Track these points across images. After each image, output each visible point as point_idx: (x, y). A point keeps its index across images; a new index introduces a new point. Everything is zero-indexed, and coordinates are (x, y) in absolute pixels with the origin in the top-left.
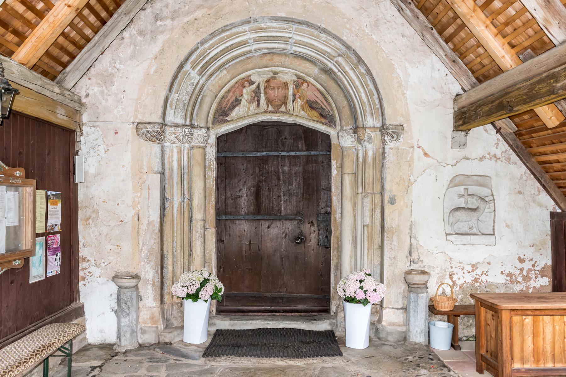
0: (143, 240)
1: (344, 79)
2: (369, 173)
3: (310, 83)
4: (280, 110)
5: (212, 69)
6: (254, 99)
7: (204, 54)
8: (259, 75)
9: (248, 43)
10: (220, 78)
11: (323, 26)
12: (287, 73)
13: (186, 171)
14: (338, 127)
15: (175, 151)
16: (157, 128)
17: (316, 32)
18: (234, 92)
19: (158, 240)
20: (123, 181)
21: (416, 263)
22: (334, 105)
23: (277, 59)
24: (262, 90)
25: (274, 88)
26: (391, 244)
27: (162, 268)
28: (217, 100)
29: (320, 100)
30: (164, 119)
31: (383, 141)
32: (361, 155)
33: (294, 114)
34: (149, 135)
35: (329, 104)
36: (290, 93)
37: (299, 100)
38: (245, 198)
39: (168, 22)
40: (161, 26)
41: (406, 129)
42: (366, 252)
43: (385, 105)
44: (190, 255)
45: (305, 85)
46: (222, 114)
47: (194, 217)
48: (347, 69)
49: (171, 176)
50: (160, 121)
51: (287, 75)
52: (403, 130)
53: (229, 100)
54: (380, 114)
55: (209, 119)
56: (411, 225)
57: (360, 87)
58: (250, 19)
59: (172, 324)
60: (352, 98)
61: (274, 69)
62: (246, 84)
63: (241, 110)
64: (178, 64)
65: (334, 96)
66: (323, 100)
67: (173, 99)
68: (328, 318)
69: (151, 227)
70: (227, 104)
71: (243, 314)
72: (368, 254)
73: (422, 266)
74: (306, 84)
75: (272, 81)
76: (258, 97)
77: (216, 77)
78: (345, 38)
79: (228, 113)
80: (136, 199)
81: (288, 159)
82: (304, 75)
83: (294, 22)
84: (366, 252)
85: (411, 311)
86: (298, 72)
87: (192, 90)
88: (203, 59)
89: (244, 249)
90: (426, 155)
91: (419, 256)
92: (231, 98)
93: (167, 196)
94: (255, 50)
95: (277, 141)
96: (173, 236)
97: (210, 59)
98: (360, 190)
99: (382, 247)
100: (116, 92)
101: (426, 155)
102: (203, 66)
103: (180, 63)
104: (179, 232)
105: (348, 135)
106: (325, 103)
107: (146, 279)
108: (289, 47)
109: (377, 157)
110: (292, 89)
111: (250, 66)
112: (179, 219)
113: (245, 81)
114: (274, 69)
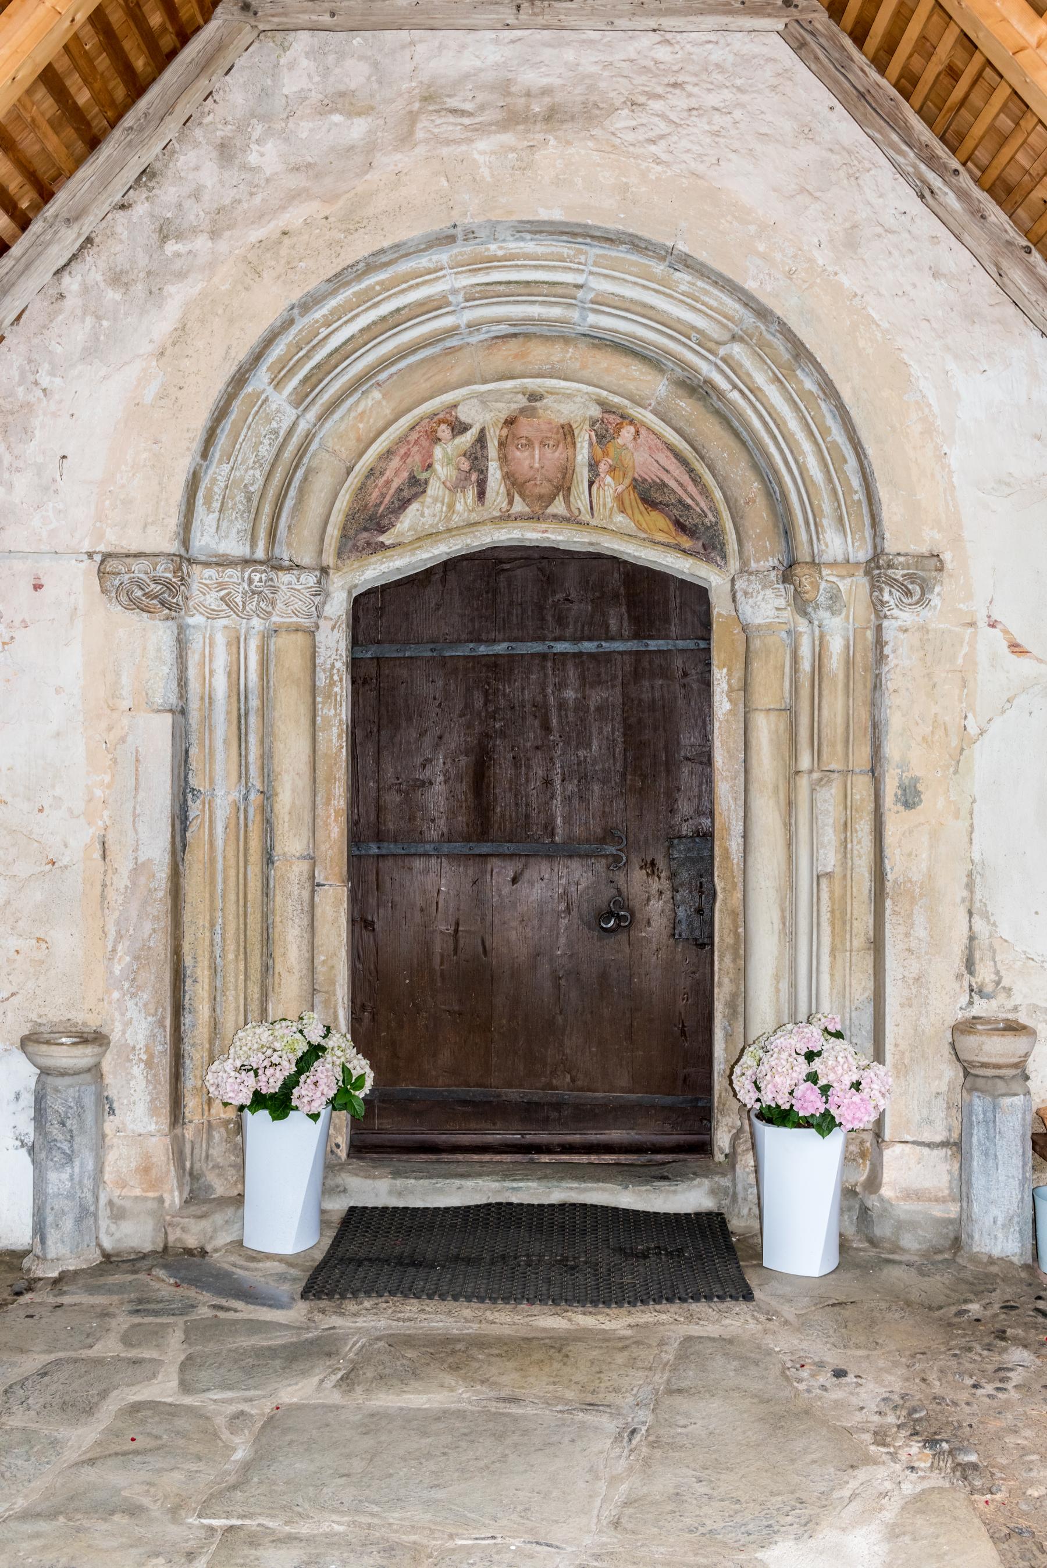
0: (118, 923)
1: (750, 412)
2: (834, 708)
3: (643, 424)
4: (552, 510)
6: (467, 479)
7: (311, 341)
8: (482, 402)
9: (449, 304)
10: (363, 412)
11: (682, 247)
12: (570, 396)
13: (254, 703)
14: (734, 564)
15: (220, 640)
16: (164, 570)
17: (659, 268)
18: (407, 455)
19: (166, 922)
20: (58, 734)
21: (988, 997)
22: (718, 495)
23: (539, 353)
24: (492, 451)
26: (907, 935)
27: (178, 1009)
29: (675, 477)
30: (186, 543)
31: (877, 606)
32: (805, 651)
33: (593, 522)
34: (139, 593)
35: (705, 491)
36: (579, 458)
37: (609, 479)
38: (439, 787)
39: (201, 243)
40: (178, 255)
41: (949, 565)
42: (826, 959)
43: (883, 493)
44: (267, 969)
46: (367, 527)
47: (278, 850)
48: (760, 379)
49: (207, 719)
50: (173, 547)
52: (940, 569)
53: (388, 482)
54: (867, 521)
55: (327, 540)
56: (970, 875)
57: (800, 436)
58: (452, 231)
59: (209, 1188)
60: (776, 472)
62: (444, 432)
63: (426, 511)
64: (229, 370)
65: (719, 465)
66: (685, 479)
67: (214, 481)
68: (707, 1172)
69: (142, 880)
70: (383, 495)
71: (433, 1157)
72: (832, 968)
73: (1010, 1004)
74: (632, 429)
75: (523, 420)
76: (481, 472)
77: (350, 410)
78: (751, 285)
80: (98, 793)
81: (576, 665)
82: (626, 402)
83: (592, 237)
84: (826, 959)
85: (976, 1153)
86: (605, 393)
87: (274, 450)
88: (308, 356)
89: (438, 950)
90: (1015, 648)
91: (997, 973)
92: (396, 475)
93: (193, 782)
94: (469, 326)
95: (541, 608)
96: (212, 909)
97: (331, 354)
98: (805, 762)
99: (877, 945)
100: (40, 459)
101: (1015, 648)
102: (306, 379)
103: (234, 368)
104: (232, 897)
105: (764, 587)
106: (691, 488)
107: (127, 1045)
108: (575, 315)
109: (858, 658)
110: (586, 445)
111: (456, 374)
112: (231, 854)
113: (440, 422)
114: (532, 384)
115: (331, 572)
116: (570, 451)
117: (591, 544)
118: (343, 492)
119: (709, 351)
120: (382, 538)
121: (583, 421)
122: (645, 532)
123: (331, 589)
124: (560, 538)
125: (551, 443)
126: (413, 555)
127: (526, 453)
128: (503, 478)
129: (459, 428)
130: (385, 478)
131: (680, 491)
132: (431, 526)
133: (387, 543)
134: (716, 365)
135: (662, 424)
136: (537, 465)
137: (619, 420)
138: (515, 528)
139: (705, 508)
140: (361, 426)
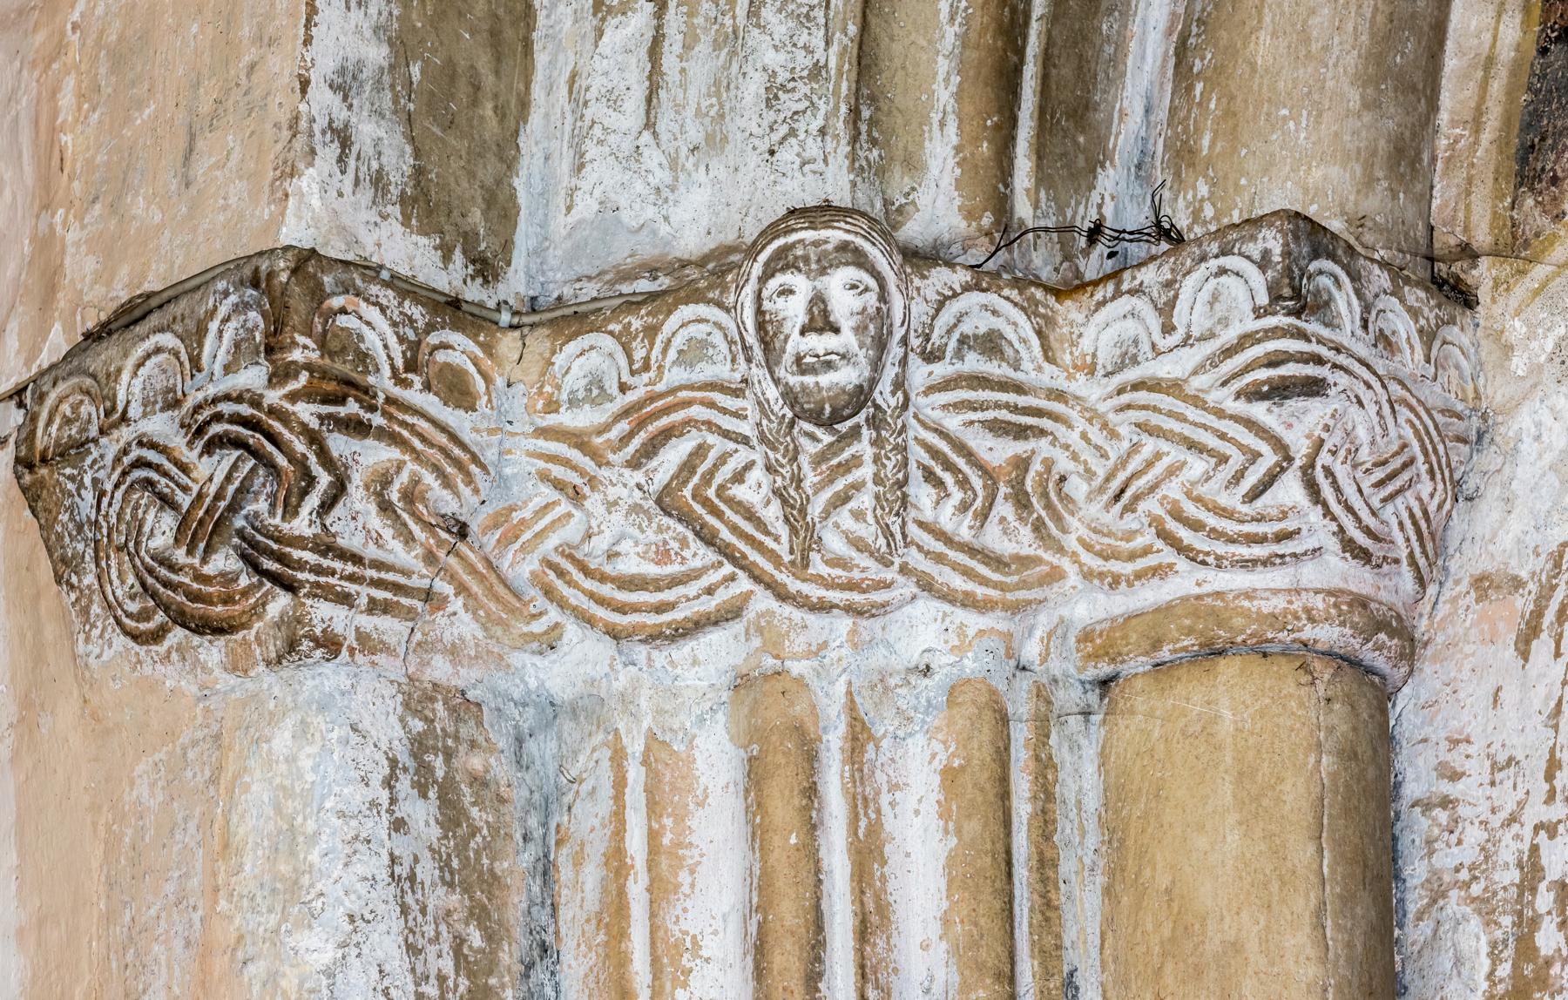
115: (1483, 275)
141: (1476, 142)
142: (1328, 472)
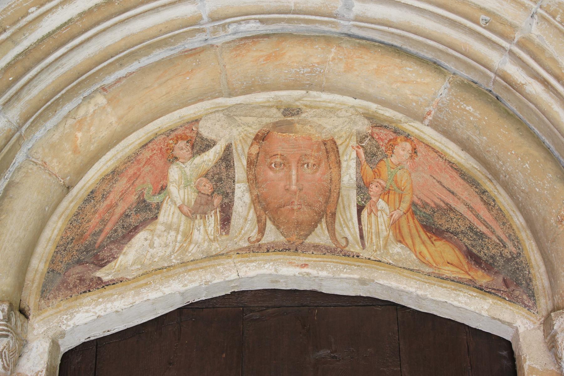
3: (421, 141)
4: (312, 239)
5: (48, 81)
8: (228, 116)
12: (333, 111)
18: (136, 176)
22: (518, 220)
23: (296, 56)
25: (285, 163)
28: (69, 205)
29: (464, 201)
33: (365, 254)
35: (501, 217)
37: (382, 204)
45: (403, 150)
51: (336, 116)
53: (112, 207)
55: (30, 276)
61: (285, 95)
63: (157, 241)
66: (476, 203)
70: (104, 222)
74: (408, 146)
75: (277, 135)
76: (227, 195)
79: (104, 254)
82: (399, 116)
86: (373, 107)
94: (213, 19)
106: (484, 212)
110: (353, 164)
111: (197, 80)
113: (177, 139)
114: (285, 95)
115: (32, 313)
116: (334, 170)
117: (363, 282)
118: (54, 218)
119: (502, 35)
120: (99, 274)
121: (349, 137)
122: (429, 265)
123: (30, 337)
124: (324, 274)
125: (312, 162)
126: (138, 294)
127: (281, 174)
128: (253, 202)
129: (201, 145)
130: (108, 202)
131: (470, 216)
132: (162, 258)
133: (106, 279)
134: (511, 53)
135: (444, 140)
136: (294, 187)
137: (392, 136)
138: (266, 262)
139: (503, 237)
140: (79, 135)
141: (32, 286)
142: (5, 353)
